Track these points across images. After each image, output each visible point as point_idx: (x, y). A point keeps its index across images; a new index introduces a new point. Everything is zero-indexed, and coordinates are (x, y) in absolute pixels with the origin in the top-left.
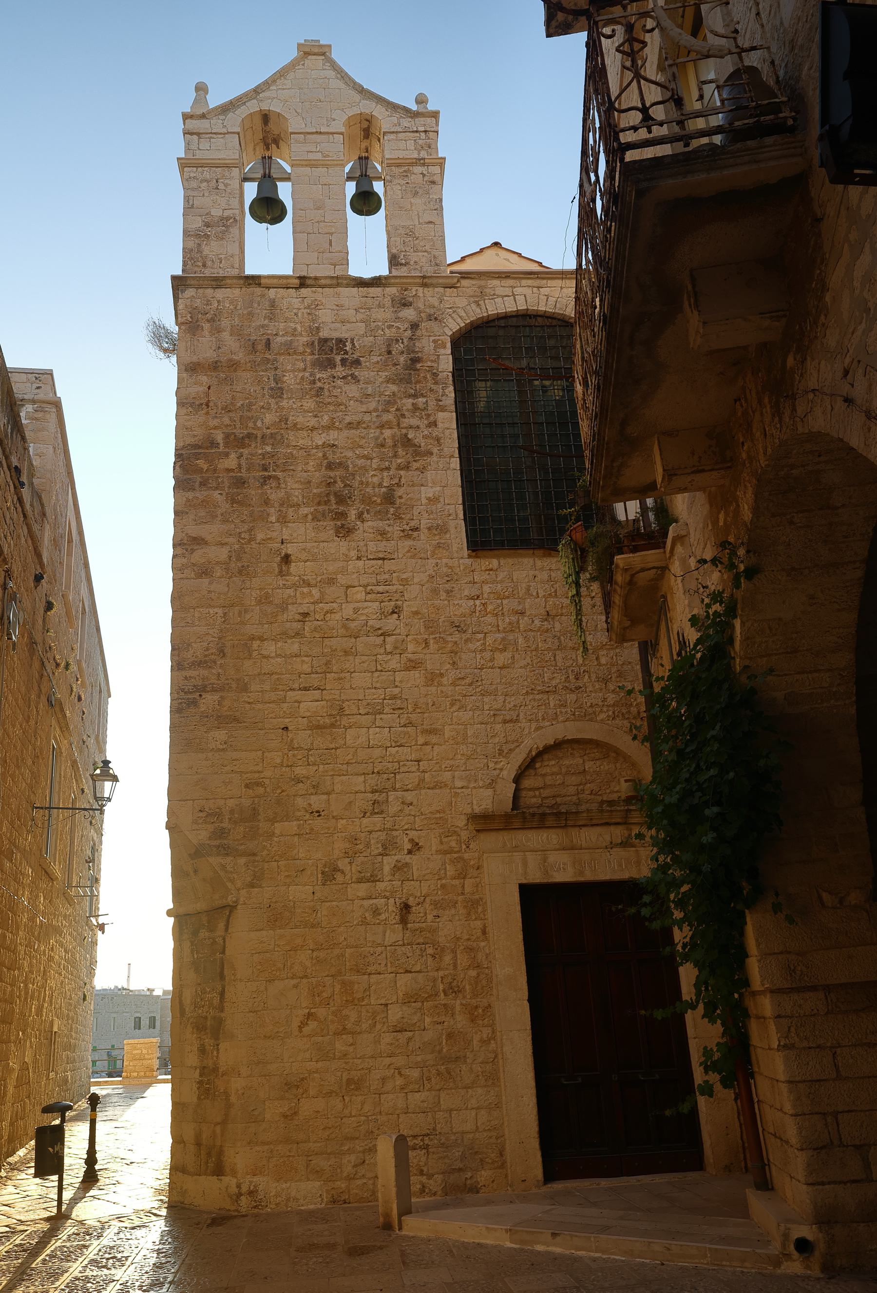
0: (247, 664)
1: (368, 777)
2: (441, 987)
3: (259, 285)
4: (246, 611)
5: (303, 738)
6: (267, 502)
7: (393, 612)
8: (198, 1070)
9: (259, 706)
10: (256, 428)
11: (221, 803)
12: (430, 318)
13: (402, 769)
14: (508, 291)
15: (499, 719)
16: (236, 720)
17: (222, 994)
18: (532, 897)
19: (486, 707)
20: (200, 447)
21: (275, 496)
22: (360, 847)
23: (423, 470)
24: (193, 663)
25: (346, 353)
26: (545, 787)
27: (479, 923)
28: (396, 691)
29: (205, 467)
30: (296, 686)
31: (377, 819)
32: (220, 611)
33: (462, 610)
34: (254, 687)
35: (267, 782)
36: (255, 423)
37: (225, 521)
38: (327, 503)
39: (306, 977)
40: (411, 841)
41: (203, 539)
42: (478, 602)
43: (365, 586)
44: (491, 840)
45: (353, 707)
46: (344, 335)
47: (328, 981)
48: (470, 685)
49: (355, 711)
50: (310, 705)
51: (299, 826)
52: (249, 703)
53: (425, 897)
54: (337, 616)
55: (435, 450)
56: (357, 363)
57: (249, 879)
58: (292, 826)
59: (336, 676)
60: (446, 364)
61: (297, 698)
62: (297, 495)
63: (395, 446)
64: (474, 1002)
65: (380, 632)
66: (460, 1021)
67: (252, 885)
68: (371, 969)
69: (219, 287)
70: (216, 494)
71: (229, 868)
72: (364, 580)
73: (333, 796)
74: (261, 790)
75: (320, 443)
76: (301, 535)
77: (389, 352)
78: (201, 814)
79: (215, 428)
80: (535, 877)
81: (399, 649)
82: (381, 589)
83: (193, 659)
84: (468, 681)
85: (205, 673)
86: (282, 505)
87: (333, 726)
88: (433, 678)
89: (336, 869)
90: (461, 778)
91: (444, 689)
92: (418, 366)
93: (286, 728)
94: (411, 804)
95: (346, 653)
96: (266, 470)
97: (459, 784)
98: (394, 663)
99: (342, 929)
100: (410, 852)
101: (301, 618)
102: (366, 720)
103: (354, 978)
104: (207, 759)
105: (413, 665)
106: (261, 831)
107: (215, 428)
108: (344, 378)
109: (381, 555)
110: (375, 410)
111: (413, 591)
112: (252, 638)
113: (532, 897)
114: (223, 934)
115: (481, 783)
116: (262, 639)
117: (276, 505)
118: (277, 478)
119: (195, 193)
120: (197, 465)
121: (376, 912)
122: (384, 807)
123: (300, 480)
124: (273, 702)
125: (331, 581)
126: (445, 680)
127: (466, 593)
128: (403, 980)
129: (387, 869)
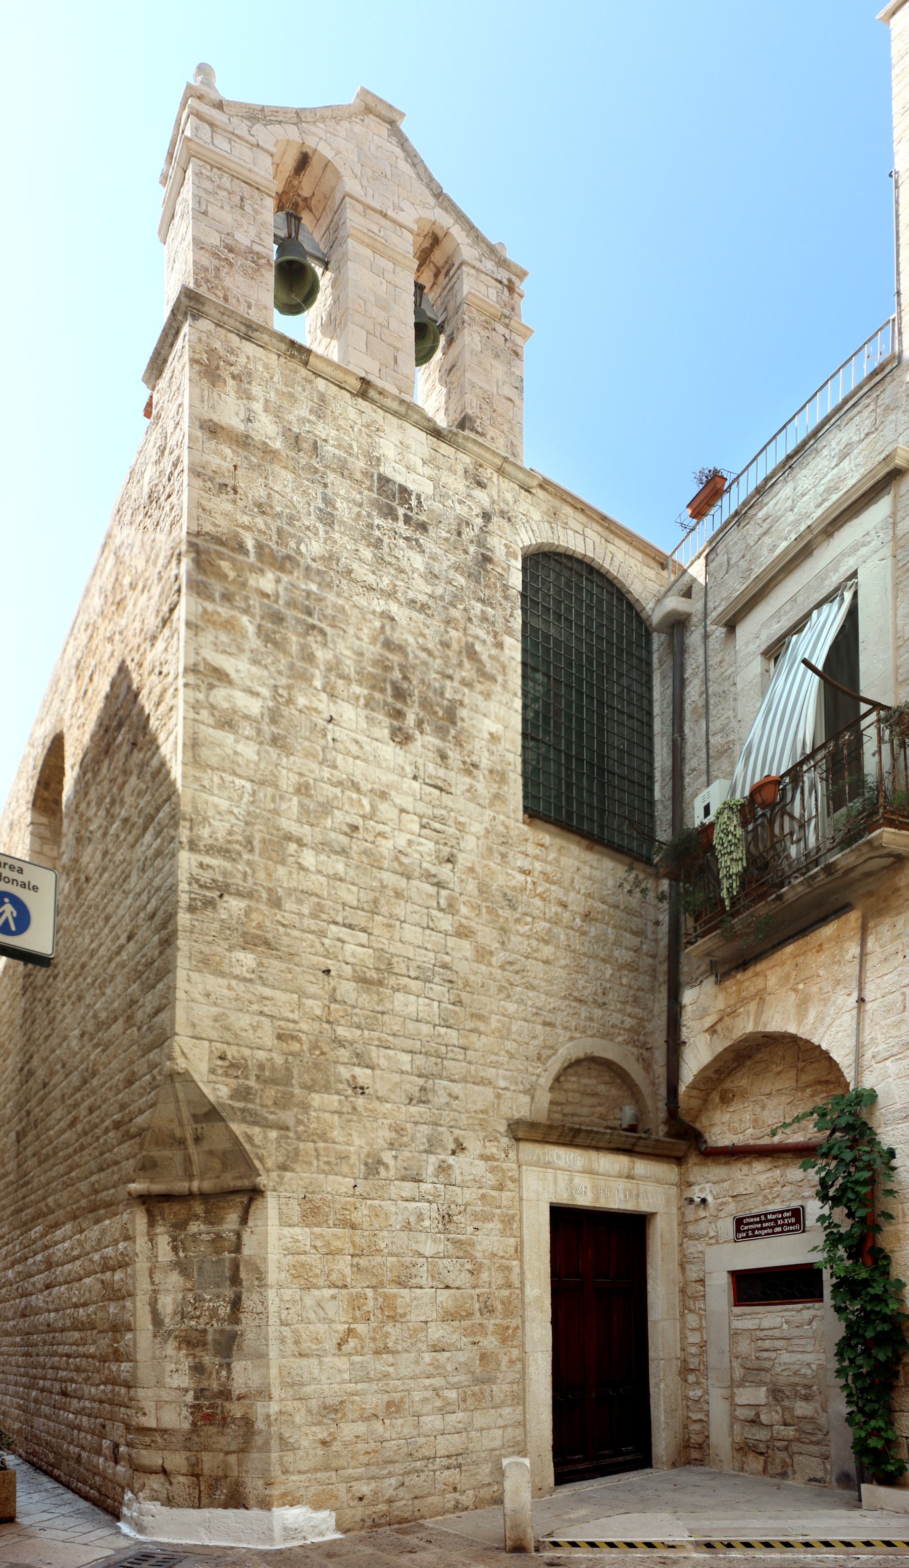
0: (281, 871)
1: (416, 1056)
2: (477, 1306)
3: (306, 364)
4: (282, 798)
5: (348, 989)
6: (310, 658)
7: (448, 861)
8: (191, 1393)
9: (295, 933)
10: (299, 552)
11: (247, 1052)
12: (502, 514)
13: (450, 1055)
14: (579, 528)
15: (540, 1019)
16: (267, 943)
17: (236, 1304)
18: (563, 1218)
19: (530, 1003)
20: (223, 544)
21: (322, 655)
22: (405, 1139)
23: (487, 696)
24: (212, 847)
25: (410, 509)
26: (568, 1103)
27: (512, 1241)
28: (447, 959)
29: (232, 574)
30: (339, 919)
31: (422, 1108)
32: (248, 785)
33: (514, 883)
34: (289, 905)
35: (304, 1037)
36: (298, 544)
37: (255, 662)
38: (383, 690)
39: (345, 1286)
40: (456, 1140)
41: (227, 675)
42: (529, 879)
43: (421, 817)
44: (531, 1151)
45: (403, 966)
46: (411, 486)
47: (370, 1293)
48: (517, 973)
49: (404, 972)
50: (355, 950)
51: (340, 1101)
52: (283, 925)
53: (466, 1205)
54: (389, 844)
55: (500, 679)
56: (423, 527)
57: (281, 1159)
58: (333, 1100)
59: (385, 921)
60: (516, 580)
61: (341, 935)
62: (349, 666)
63: (460, 652)
64: (505, 1322)
65: (435, 880)
66: (490, 1342)
67: (283, 1168)
68: (413, 1281)
69: (247, 338)
70: (245, 619)
71: (257, 1141)
72: (422, 808)
73: (378, 1072)
74: (296, 1047)
75: (378, 609)
76: (353, 719)
77: (459, 534)
78: (220, 1062)
79: (248, 528)
80: (564, 1198)
81: (451, 908)
82: (437, 826)
83: (210, 841)
84: (515, 967)
85: (228, 865)
86: (329, 670)
87: (380, 983)
88: (482, 954)
89: (380, 1162)
90: (505, 1078)
91: (493, 970)
92: (489, 567)
93: (327, 972)
94: (457, 1098)
95: (398, 894)
96: (310, 614)
97: (502, 1084)
98: (446, 923)
99: (385, 1233)
100: (453, 1153)
101: (348, 831)
102: (414, 985)
103: (395, 1291)
104: (230, 988)
105: (463, 933)
106: (295, 1100)
107: (248, 528)
108: (407, 539)
109: (440, 783)
110: (442, 598)
111: (470, 842)
112: (289, 838)
113: (563, 1218)
114: (235, 1226)
115: (521, 1087)
116: (300, 842)
117: (322, 667)
118: (323, 633)
119: (211, 199)
120: (219, 567)
121: (420, 1217)
122: (430, 1096)
123: (353, 645)
124: (312, 932)
125: (383, 795)
126: (494, 960)
127: (519, 863)
128: (444, 1296)
129: (431, 1169)
